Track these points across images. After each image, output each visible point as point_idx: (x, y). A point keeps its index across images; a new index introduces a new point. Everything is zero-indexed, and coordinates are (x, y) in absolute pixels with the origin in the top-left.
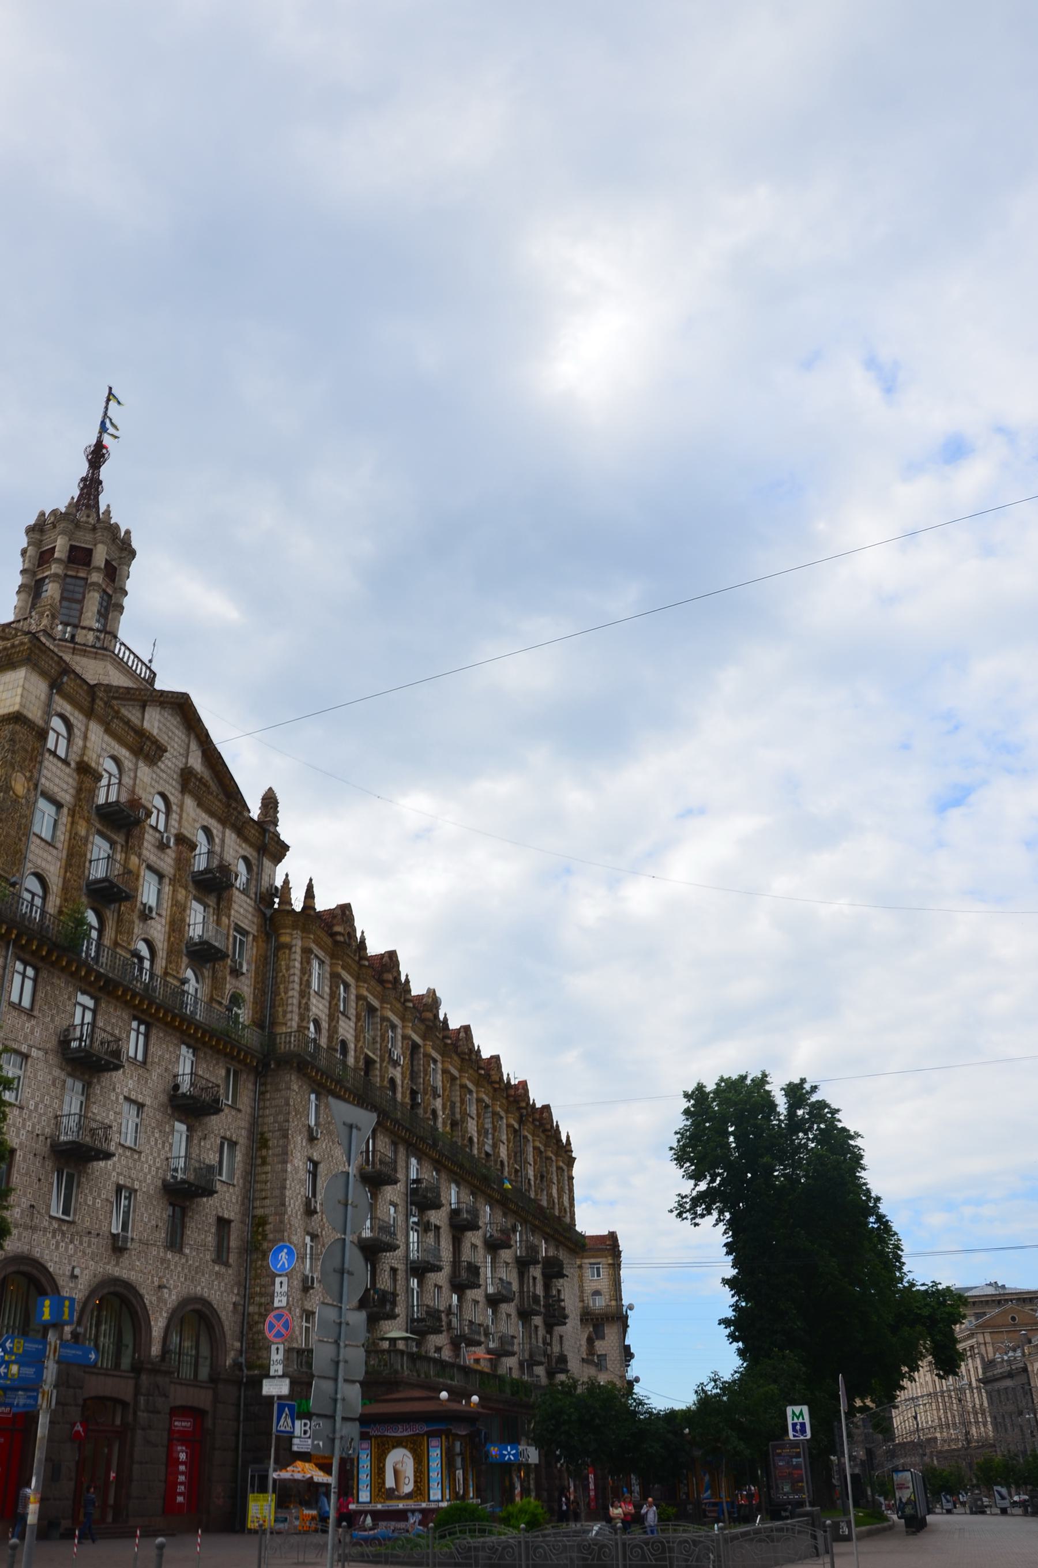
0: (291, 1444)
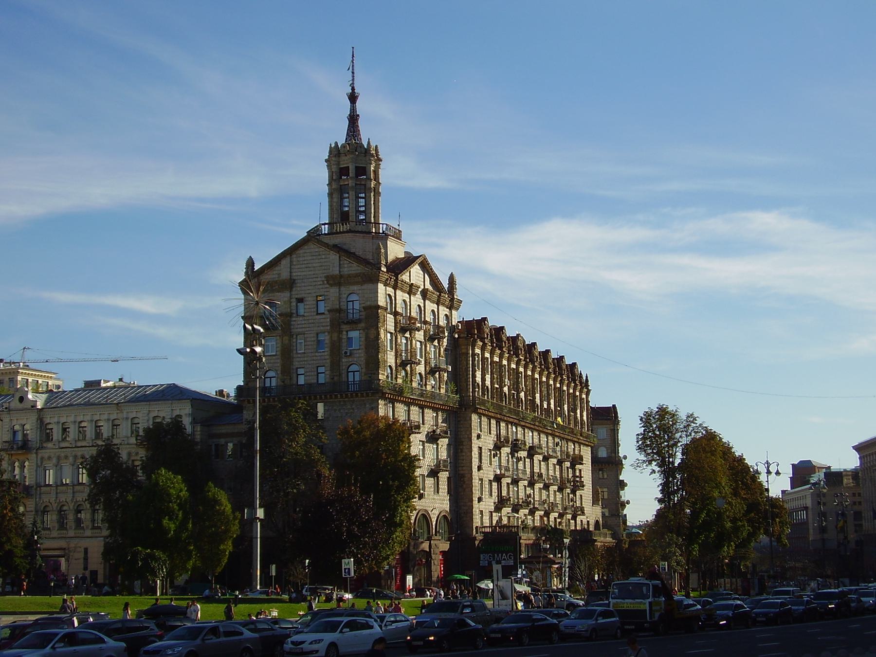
0: (480, 563)
